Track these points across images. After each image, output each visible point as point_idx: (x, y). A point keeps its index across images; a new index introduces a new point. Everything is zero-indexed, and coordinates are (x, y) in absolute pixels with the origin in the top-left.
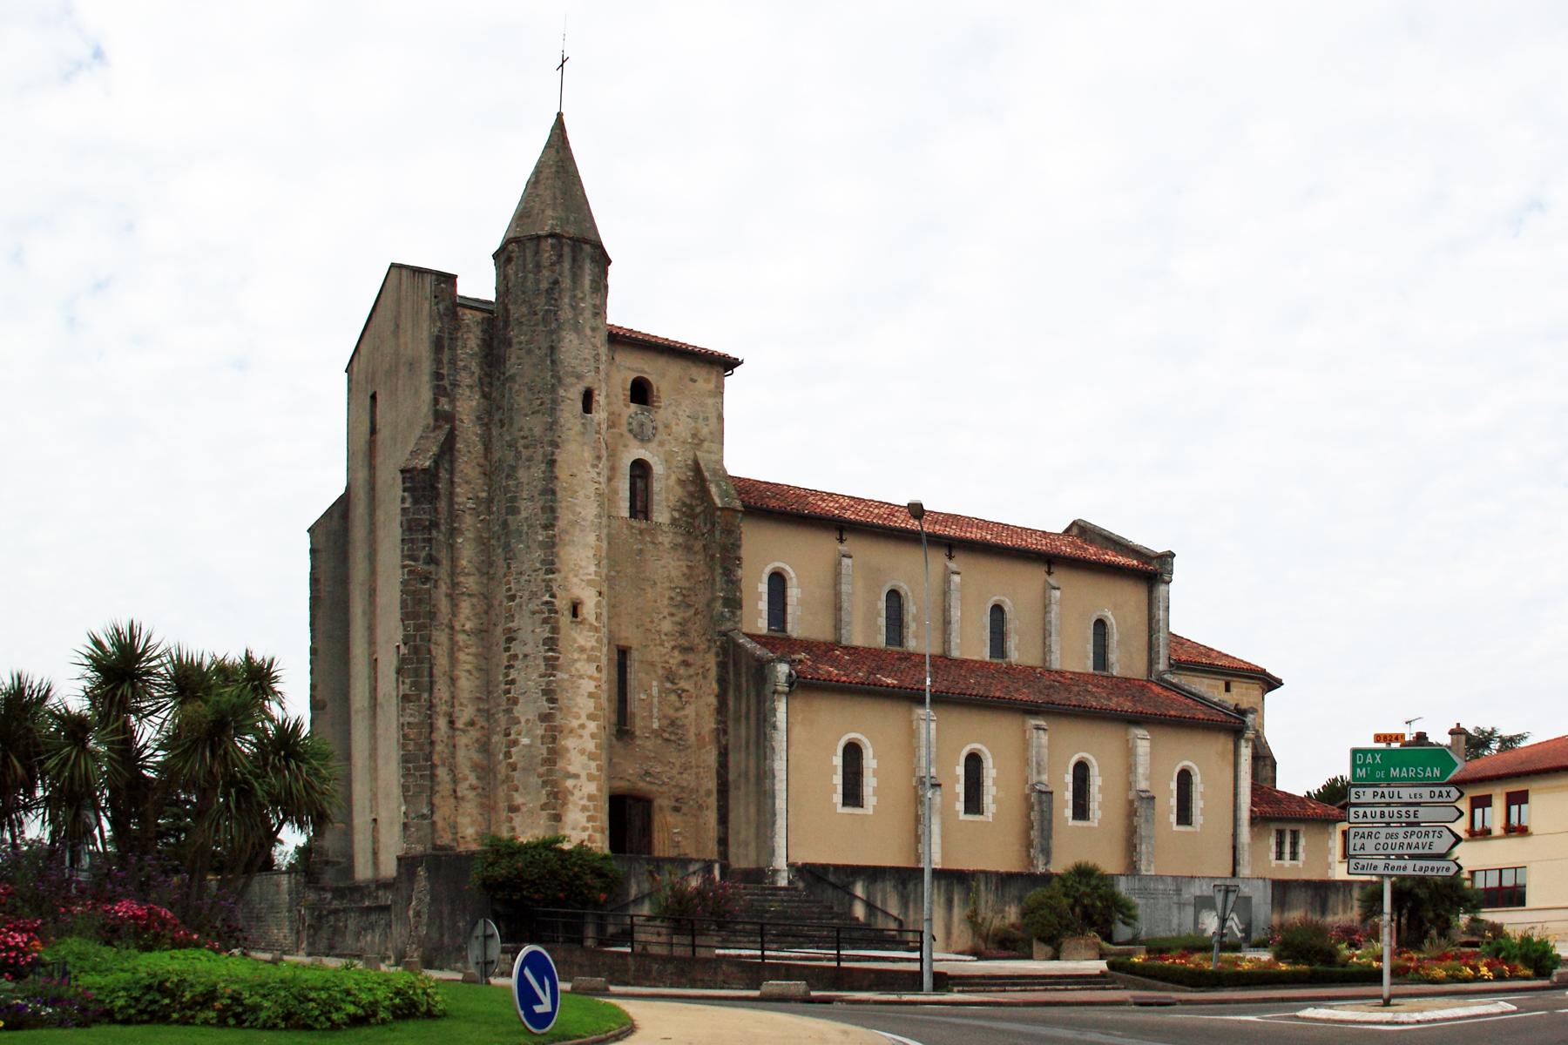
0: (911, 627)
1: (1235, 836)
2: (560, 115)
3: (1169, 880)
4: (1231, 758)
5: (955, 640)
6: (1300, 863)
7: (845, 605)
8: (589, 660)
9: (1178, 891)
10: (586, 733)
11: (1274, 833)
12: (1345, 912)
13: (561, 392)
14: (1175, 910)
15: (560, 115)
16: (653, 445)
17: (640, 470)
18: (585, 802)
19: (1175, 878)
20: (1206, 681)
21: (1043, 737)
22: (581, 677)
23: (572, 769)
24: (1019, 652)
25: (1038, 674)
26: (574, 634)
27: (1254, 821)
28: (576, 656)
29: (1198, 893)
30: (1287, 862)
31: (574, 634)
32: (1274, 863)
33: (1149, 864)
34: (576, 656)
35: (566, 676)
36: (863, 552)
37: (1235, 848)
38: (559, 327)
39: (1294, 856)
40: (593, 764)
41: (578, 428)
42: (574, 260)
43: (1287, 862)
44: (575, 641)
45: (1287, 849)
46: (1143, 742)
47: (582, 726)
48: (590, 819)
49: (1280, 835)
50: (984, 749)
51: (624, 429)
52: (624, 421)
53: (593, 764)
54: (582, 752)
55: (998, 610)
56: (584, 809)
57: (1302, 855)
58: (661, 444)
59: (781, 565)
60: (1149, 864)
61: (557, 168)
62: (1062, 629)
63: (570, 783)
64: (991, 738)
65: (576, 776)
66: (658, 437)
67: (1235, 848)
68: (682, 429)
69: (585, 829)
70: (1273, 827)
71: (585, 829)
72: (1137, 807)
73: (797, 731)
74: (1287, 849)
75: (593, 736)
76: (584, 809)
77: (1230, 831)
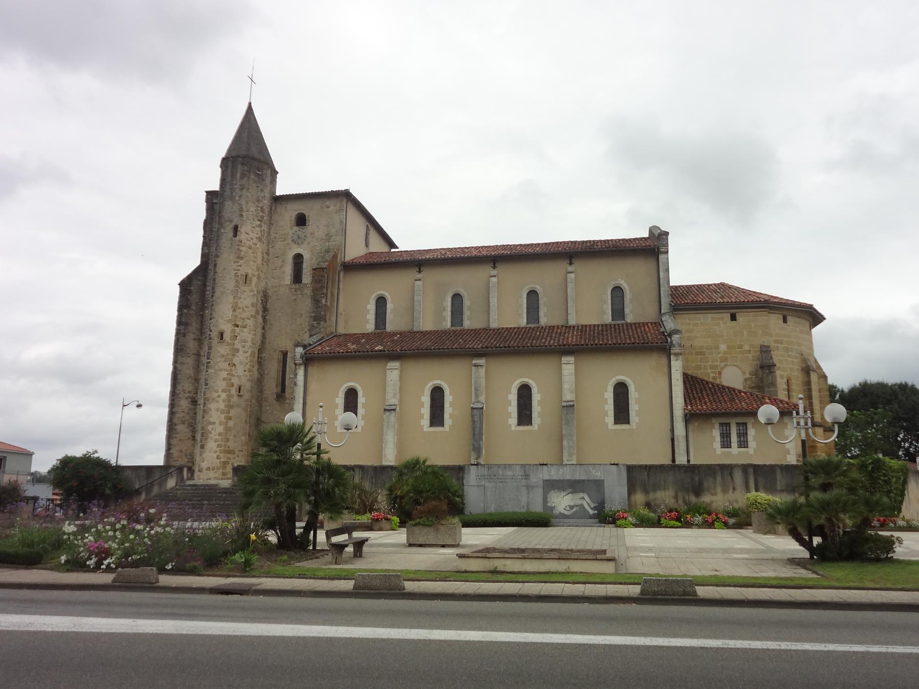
0: (467, 313)
1: (672, 430)
2: (250, 104)
3: (518, 468)
4: (666, 370)
5: (494, 316)
6: (751, 450)
7: (416, 308)
8: (225, 361)
9: (526, 476)
10: (220, 400)
11: (717, 426)
12: (725, 491)
13: (222, 231)
14: (524, 491)
15: (250, 104)
16: (305, 245)
17: (298, 258)
18: (217, 437)
19: (523, 466)
20: (710, 316)
21: (480, 370)
22: (220, 370)
23: (212, 420)
24: (545, 319)
25: (411, 335)
26: (219, 349)
27: (689, 418)
28: (219, 359)
29: (546, 477)
30: (735, 449)
31: (219, 349)
32: (719, 450)
33: (570, 455)
34: (219, 359)
35: (213, 371)
36: (431, 276)
37: (673, 440)
38: (224, 200)
39: (743, 444)
40: (223, 416)
41: (229, 245)
42: (233, 167)
43: (735, 449)
44: (219, 352)
45: (734, 438)
46: (393, 371)
47: (219, 396)
48: (219, 446)
49: (725, 427)
50: (431, 384)
51: (290, 241)
52: (290, 236)
53: (223, 416)
54: (218, 410)
55: (532, 294)
56: (216, 441)
57: (752, 443)
58: (309, 243)
59: (382, 292)
60: (570, 455)
61: (249, 129)
62: (586, 302)
63: (210, 427)
64: (449, 376)
65: (214, 423)
66: (307, 240)
67: (673, 440)
68: (321, 233)
69: (216, 452)
70: (716, 422)
71: (216, 452)
72: (476, 418)
73: (312, 387)
74: (734, 438)
75: (224, 401)
76: (216, 441)
77: (669, 427)
